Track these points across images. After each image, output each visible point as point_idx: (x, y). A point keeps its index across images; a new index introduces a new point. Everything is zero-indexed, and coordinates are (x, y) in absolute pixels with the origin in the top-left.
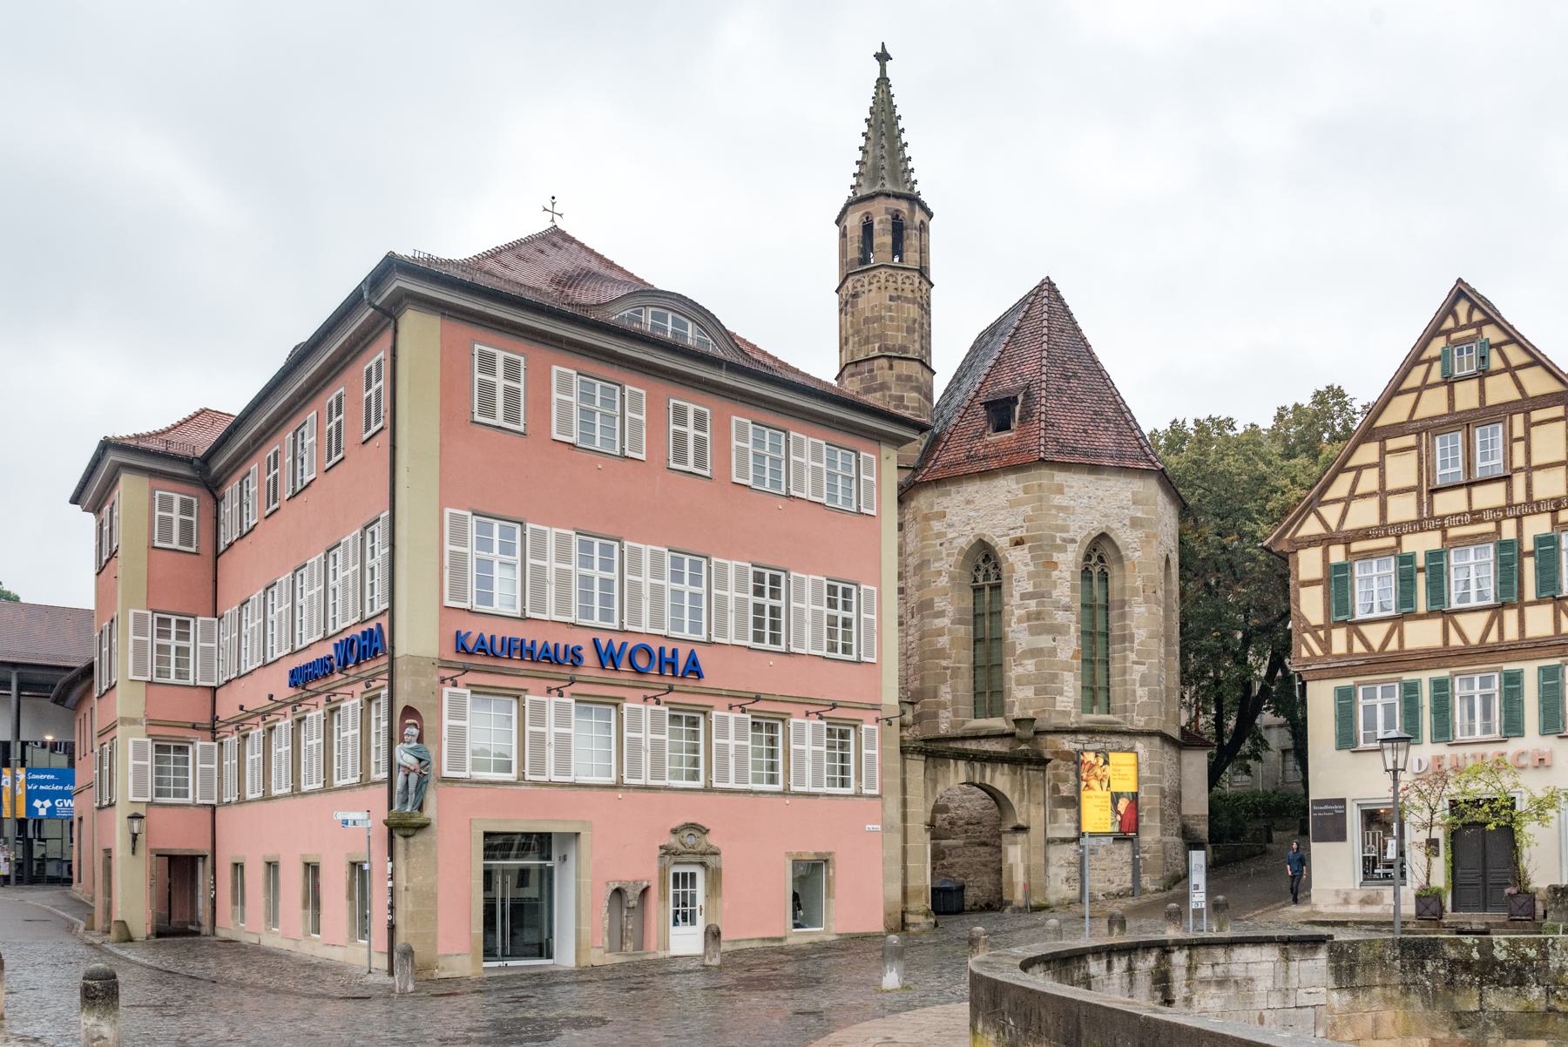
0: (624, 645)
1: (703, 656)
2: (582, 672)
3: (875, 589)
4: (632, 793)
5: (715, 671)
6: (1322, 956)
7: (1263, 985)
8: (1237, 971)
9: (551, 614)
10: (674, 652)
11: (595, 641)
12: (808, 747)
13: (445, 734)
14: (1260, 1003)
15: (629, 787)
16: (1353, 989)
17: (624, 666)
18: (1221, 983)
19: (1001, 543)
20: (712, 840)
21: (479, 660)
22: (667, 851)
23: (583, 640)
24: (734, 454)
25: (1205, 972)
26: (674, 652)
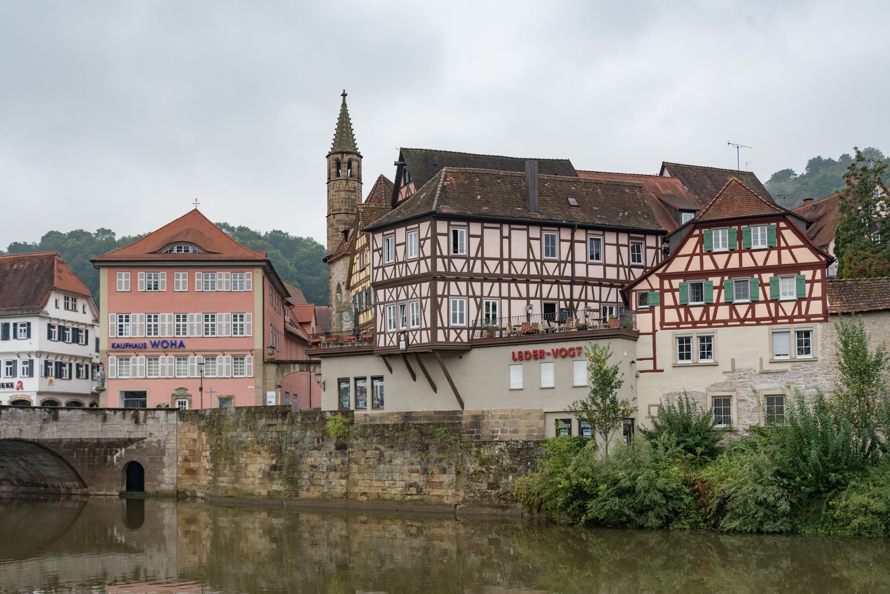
0: (159, 341)
1: (185, 342)
2: (147, 349)
3: (251, 314)
4: (163, 380)
5: (188, 345)
6: (175, 414)
7: (162, 419)
8: (156, 416)
9: (138, 335)
10: (176, 341)
11: (151, 341)
12: (224, 364)
13: (109, 368)
14: (161, 423)
15: (161, 378)
16: (183, 421)
17: (160, 347)
18: (153, 418)
19: (341, 283)
20: (189, 392)
21: (118, 349)
22: (173, 395)
23: (147, 342)
24: (196, 283)
25: (149, 416)
26: (176, 341)
